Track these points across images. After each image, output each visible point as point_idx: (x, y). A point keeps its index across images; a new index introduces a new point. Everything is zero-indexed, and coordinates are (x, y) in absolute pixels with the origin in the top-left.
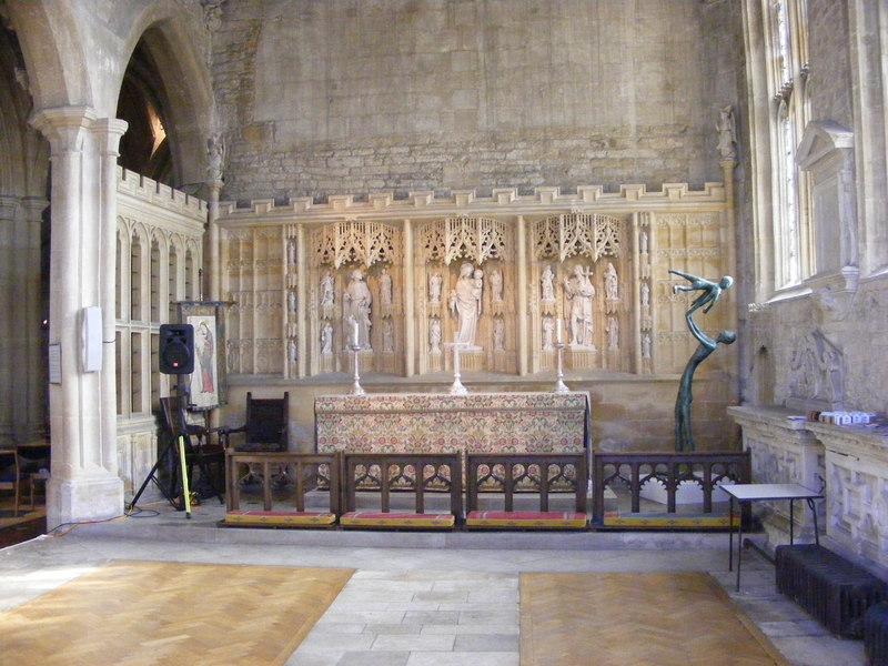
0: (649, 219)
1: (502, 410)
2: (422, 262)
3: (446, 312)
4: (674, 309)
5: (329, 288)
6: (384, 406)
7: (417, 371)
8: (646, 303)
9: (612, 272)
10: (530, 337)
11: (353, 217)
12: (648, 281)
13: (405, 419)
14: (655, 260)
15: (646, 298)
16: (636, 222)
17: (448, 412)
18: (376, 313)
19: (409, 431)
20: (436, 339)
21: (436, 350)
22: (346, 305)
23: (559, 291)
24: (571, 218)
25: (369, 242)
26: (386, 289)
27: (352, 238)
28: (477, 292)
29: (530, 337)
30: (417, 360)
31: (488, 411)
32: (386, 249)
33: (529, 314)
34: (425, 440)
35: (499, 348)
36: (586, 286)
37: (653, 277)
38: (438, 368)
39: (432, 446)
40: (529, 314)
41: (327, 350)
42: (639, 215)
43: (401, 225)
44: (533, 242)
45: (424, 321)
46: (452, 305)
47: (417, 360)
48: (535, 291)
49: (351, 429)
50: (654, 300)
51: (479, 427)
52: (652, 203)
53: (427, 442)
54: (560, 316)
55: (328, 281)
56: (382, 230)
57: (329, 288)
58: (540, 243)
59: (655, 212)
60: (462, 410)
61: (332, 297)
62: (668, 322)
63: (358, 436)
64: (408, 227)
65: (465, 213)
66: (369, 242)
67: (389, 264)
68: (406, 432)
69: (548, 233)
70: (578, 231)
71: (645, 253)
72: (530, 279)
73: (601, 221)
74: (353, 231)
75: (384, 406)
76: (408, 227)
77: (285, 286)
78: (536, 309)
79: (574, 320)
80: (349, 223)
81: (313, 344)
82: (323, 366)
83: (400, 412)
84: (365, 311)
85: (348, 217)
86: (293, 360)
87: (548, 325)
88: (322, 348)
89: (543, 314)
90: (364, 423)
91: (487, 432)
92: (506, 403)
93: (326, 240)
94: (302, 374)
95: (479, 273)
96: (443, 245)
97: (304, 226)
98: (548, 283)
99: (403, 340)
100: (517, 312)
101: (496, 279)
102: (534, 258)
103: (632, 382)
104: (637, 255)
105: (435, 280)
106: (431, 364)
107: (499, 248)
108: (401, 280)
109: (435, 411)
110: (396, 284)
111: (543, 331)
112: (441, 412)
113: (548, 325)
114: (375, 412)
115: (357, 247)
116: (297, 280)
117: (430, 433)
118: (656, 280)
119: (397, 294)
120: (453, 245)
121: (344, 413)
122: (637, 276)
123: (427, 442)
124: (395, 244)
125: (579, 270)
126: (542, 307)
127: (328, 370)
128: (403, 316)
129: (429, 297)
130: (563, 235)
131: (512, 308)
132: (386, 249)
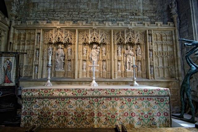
0: (152, 32)
1: (125, 97)
2: (81, 43)
3: (88, 59)
4: (159, 59)
5: (51, 50)
6: (61, 94)
7: (78, 77)
8: (151, 57)
9: (139, 48)
10: (114, 67)
11: (59, 27)
13: (73, 101)
14: (153, 44)
15: (151, 55)
16: (148, 33)
17: (97, 97)
18: (66, 59)
19: (75, 107)
20: (85, 67)
21: (85, 70)
22: (56, 56)
23: (123, 54)
24: (128, 30)
25: (64, 36)
26: (69, 51)
27: (59, 34)
28: (98, 53)
29: (114, 67)
30: (79, 73)
31: (117, 97)
32: (70, 38)
34: (83, 113)
35: (104, 70)
36: (131, 52)
37: (154, 49)
38: (85, 76)
39: (87, 117)
40: (114, 60)
42: (149, 30)
43: (75, 31)
44: (116, 39)
45: (81, 61)
46: (90, 56)
47: (79, 73)
48: (116, 53)
49: (42, 107)
50: (154, 56)
51: (113, 106)
52: (152, 27)
53: (85, 115)
54: (123, 61)
55: (50, 47)
56: (69, 33)
57: (51, 50)
58: (117, 39)
59: (153, 30)
60: (104, 97)
61: (52, 53)
62: (157, 64)
63: (46, 111)
64: (77, 31)
65: (95, 27)
66: (64, 36)
67: (71, 44)
68: (73, 109)
69: (120, 35)
70: (130, 34)
71: (150, 42)
72: (114, 49)
73: (137, 32)
74: (59, 32)
75: (61, 94)
76: (77, 31)
77: (35, 48)
78: (116, 58)
79: (127, 62)
80: (58, 29)
81: (44, 68)
83: (70, 97)
84: (62, 58)
85: (58, 27)
86: (36, 73)
87: (119, 64)
89: (118, 60)
90: (49, 103)
91: (118, 109)
92: (128, 93)
95: (99, 47)
96: (88, 38)
97: (43, 30)
98: (120, 51)
99: (74, 67)
100: (111, 60)
101: (104, 49)
102: (116, 43)
103: (148, 82)
105: (85, 49)
107: (105, 40)
108: (74, 48)
109: (89, 97)
110: (73, 50)
111: (118, 65)
112: (92, 97)
113: (119, 64)
114: (56, 98)
116: (40, 46)
117: (86, 109)
118: (154, 50)
119: (73, 53)
120: (91, 38)
121: (39, 98)
122: (148, 49)
123: (85, 115)
124: (73, 38)
125: (129, 47)
126: (118, 58)
128: (74, 60)
129: (83, 54)
130: (126, 35)
131: (109, 58)
132: (70, 38)
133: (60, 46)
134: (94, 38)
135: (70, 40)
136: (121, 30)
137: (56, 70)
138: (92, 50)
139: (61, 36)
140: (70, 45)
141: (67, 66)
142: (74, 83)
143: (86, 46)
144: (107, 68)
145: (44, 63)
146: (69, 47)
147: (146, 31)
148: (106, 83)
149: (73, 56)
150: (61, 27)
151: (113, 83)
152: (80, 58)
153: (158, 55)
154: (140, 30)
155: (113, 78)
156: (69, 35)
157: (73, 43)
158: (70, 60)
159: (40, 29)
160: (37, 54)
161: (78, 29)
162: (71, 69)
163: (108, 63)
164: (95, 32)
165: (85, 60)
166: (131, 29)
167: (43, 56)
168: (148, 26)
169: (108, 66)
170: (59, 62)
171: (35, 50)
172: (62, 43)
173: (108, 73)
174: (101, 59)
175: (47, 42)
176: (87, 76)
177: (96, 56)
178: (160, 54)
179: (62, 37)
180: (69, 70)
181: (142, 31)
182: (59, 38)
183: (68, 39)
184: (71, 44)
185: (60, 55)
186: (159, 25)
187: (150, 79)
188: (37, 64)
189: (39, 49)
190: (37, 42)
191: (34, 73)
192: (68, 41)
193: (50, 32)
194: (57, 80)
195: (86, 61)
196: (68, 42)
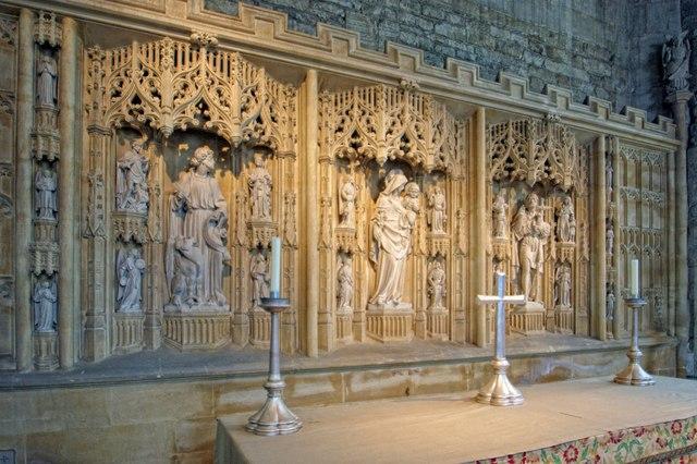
7: (322, 347)
12: (611, 223)
16: (603, 148)
25: (235, 95)
33: (323, 248)
35: (438, 307)
38: (349, 339)
41: (130, 308)
42: (607, 138)
45: (332, 255)
77: (26, 155)
80: (196, 45)
82: (122, 334)
86: (47, 329)
88: (119, 302)
93: (136, 72)
94: (70, 360)
97: (81, 26)
101: (439, 199)
104: (604, 191)
106: (340, 334)
120: (390, 132)
127: (134, 347)
134: (405, 139)
136: (518, 116)
137: (185, 309)
138: (383, 199)
142: (306, 380)
143: (348, 171)
144: (455, 298)
145: (98, 259)
147: (596, 141)
148: (458, 365)
151: (483, 364)
152: (98, 223)
153: (626, 243)
154: (580, 132)
155: (314, 350)
157: (283, 149)
159: (59, 20)
161: (321, 74)
163: (455, 269)
164: (409, 106)
165: (133, 240)
166: (557, 121)
168: (607, 118)
169: (456, 285)
171: (27, 168)
172: (150, 131)
173: (459, 321)
174: (423, 247)
176: (358, 338)
177: (403, 233)
178: (632, 241)
179: (155, 94)
181: (587, 137)
182: (203, 105)
186: (638, 119)
187: (606, 341)
188: (50, 270)
190: (37, 110)
191: (27, 332)
193: (136, 55)
195: (139, 245)
196: (351, 150)
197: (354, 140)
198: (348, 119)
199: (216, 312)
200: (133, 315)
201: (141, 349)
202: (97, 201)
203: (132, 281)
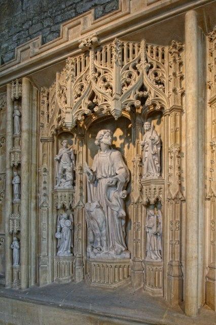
18: (135, 197)
41: (64, 252)
57: (65, 164)
61: (69, 176)
81: (44, 242)
84: (117, 195)
88: (57, 250)
99: (181, 242)
108: (177, 133)
115: (98, 87)
119: (169, 162)
124: (166, 74)
127: (65, 279)
128: (179, 199)
132: (149, 81)
133: (103, 136)
135: (152, 90)
137: (92, 255)
139: (105, 80)
140: (154, 122)
141: (141, 232)
145: (44, 221)
146: (149, 134)
149: (174, 181)
150: (100, 36)
156: (143, 66)
158: (157, 202)
160: (16, 186)
162: (162, 253)
167: (37, 191)
170: (99, 215)
175: (48, 133)
180: (154, 257)
183: (143, 88)
184: (157, 114)
185: (104, 183)
189: (19, 165)
192: (143, 99)
194: (90, 307)
197: (141, 93)
198: (135, 74)
199: (114, 259)
200: (65, 258)
201: (70, 280)
202: (43, 185)
203: (63, 235)
